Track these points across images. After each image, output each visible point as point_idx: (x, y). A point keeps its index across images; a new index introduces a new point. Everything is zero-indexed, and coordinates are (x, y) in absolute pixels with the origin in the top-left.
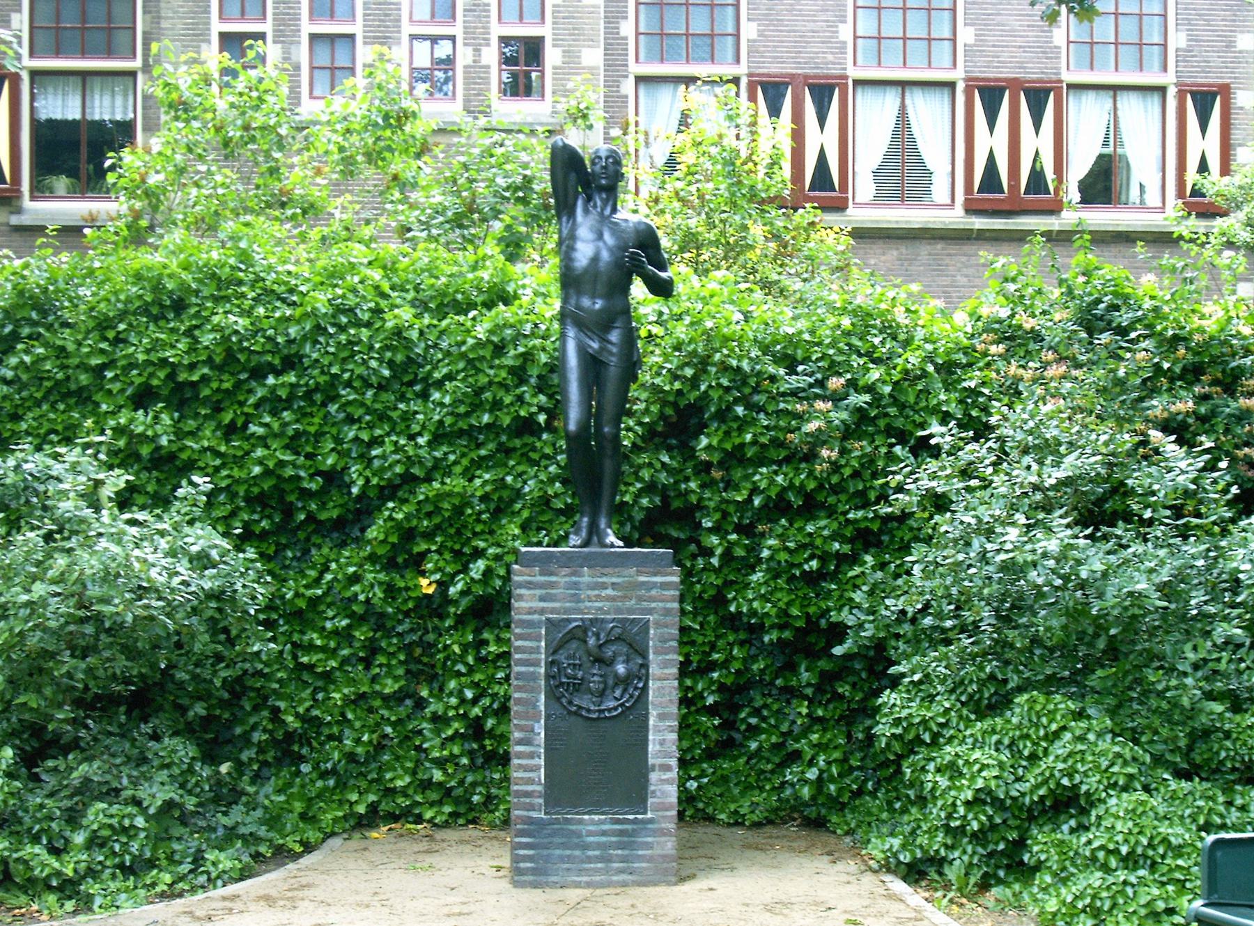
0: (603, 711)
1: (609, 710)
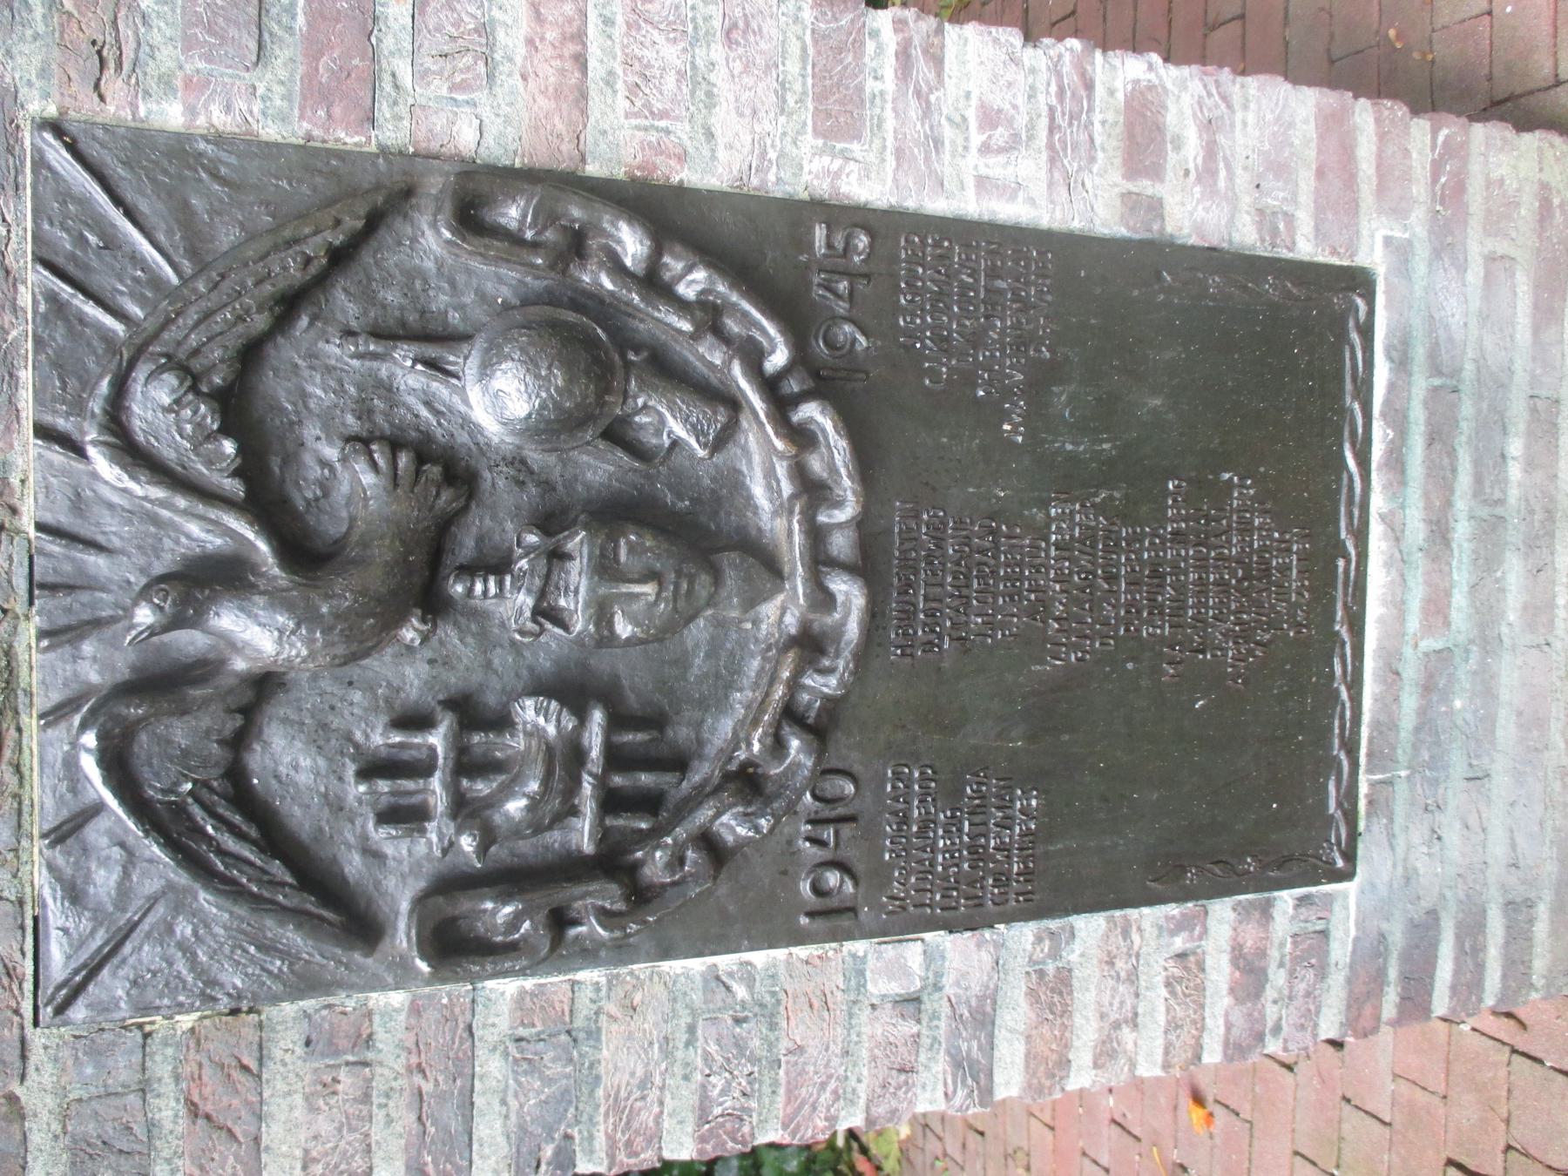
0: (816, 535)
1: (813, 492)
